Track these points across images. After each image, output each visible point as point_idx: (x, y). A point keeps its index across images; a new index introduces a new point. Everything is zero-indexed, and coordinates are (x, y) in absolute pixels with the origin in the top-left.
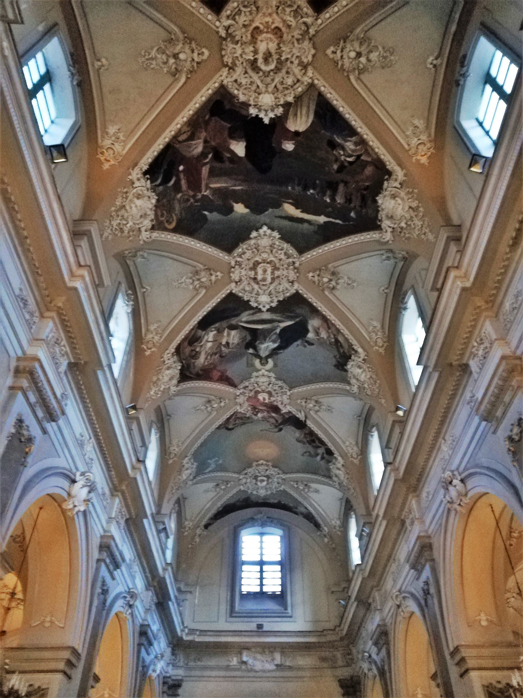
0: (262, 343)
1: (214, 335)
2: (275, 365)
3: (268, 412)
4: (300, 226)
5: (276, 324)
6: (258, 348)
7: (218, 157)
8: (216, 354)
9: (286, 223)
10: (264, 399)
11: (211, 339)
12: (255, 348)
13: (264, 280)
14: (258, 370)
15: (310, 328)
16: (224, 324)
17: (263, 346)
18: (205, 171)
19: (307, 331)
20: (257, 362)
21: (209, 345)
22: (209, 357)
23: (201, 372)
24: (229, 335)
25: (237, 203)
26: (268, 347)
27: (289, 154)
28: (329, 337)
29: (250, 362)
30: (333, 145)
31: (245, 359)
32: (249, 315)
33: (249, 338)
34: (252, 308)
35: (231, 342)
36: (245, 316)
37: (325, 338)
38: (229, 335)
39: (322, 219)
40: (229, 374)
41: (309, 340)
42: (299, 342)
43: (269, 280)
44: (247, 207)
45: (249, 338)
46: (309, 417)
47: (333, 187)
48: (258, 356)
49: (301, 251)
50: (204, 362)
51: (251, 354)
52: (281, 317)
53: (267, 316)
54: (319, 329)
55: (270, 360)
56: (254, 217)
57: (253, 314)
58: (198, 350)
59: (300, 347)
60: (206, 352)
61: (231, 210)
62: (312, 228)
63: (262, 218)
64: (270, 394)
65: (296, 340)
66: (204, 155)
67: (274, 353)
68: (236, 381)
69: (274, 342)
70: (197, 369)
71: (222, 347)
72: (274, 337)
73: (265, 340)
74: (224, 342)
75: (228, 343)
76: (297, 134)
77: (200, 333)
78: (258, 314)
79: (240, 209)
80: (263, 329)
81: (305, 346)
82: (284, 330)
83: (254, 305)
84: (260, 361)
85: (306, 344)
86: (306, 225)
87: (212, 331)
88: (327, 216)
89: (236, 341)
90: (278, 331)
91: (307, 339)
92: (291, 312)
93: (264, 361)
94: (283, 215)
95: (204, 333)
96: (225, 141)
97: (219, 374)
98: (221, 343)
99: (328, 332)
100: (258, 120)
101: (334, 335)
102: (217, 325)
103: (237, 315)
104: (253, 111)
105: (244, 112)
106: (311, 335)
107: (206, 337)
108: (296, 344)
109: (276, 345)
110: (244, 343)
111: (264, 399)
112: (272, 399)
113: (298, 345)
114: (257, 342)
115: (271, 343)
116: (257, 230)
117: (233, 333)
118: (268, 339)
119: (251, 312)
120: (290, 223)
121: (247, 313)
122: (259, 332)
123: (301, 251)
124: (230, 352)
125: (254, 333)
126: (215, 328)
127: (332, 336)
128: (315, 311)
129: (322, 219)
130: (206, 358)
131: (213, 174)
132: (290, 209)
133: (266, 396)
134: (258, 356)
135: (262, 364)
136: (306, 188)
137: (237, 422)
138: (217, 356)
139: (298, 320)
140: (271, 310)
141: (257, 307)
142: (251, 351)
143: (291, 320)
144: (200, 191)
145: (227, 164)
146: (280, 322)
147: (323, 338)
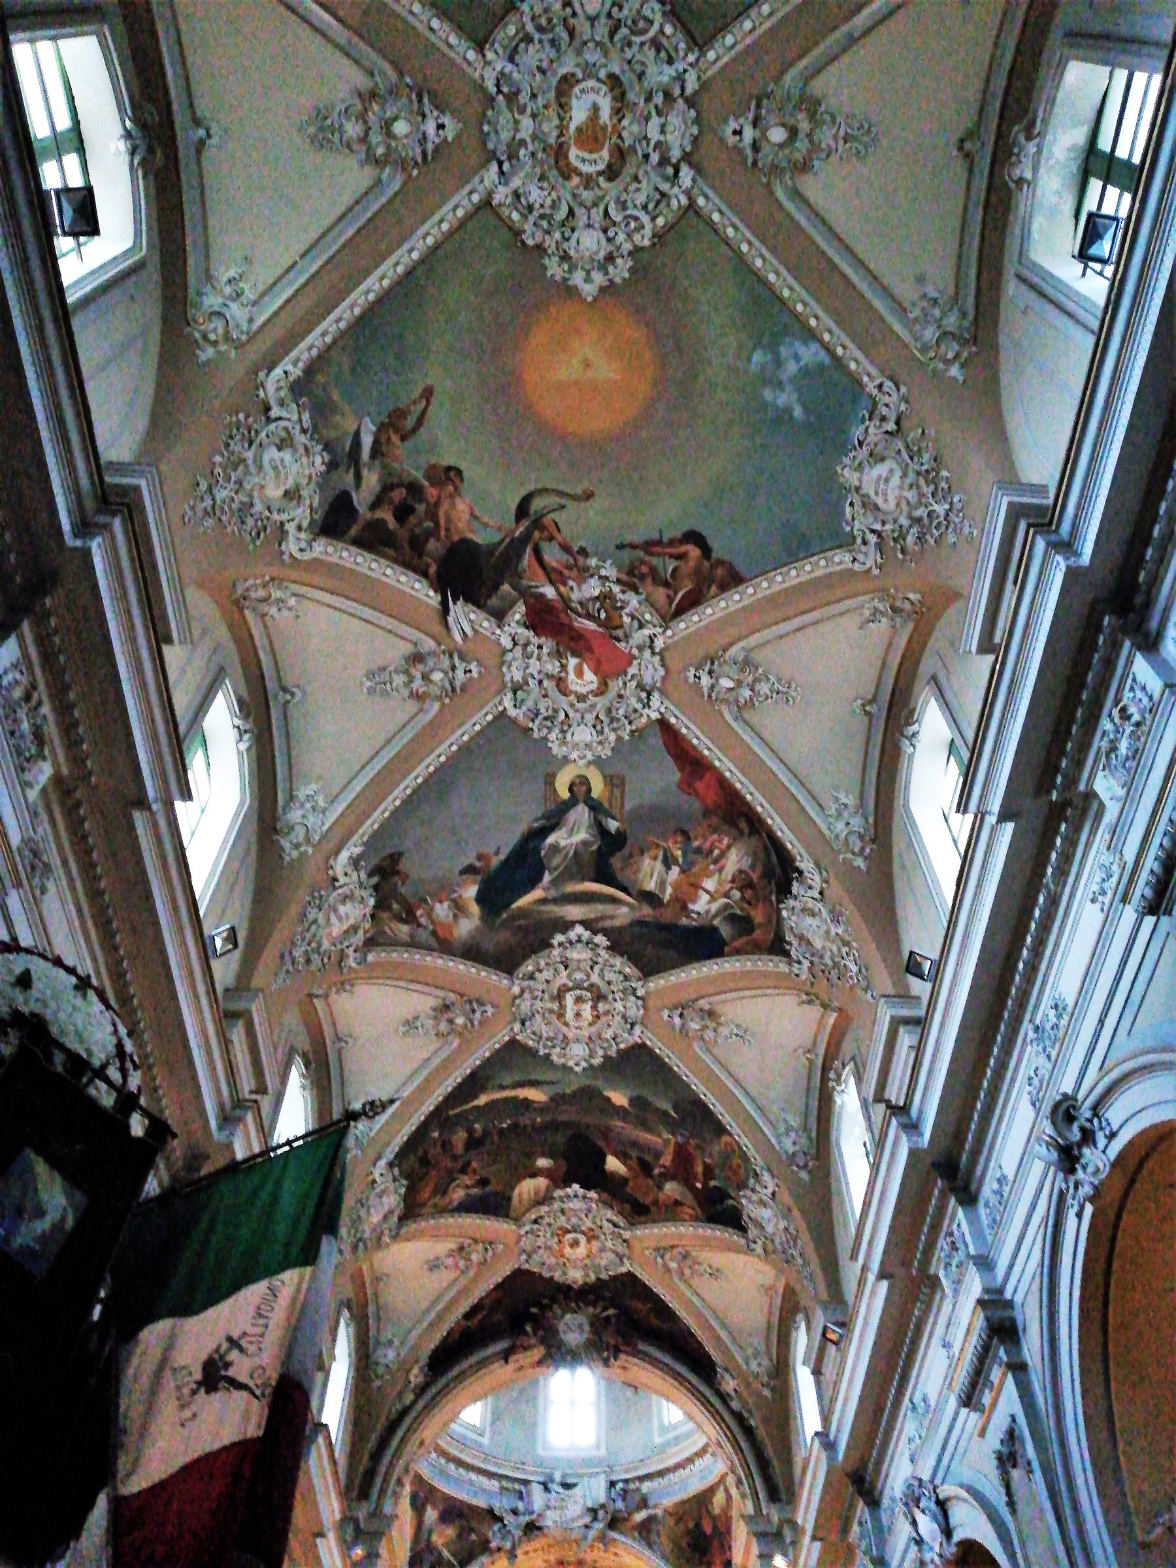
0: (585, 843)
1: (694, 902)
2: (550, 780)
3: (566, 601)
4: (517, 1078)
5: (553, 893)
6: (595, 831)
7: (645, 1168)
8: (698, 851)
9: (541, 1077)
10: (579, 673)
11: (705, 897)
12: (602, 831)
13: (579, 1000)
14: (598, 762)
15: (475, 909)
16: (667, 916)
17: (582, 835)
18: (667, 1159)
19: (480, 899)
20: (598, 788)
21: (710, 884)
22: (716, 852)
23: (743, 825)
24: (662, 884)
25: (622, 1107)
26: (570, 834)
27: (543, 1155)
28: (429, 915)
29: (617, 792)
30: (483, 1182)
31: (628, 806)
32: (612, 917)
33: (616, 862)
34: (606, 932)
35: (659, 866)
36: (622, 915)
37: (438, 905)
38: (662, 884)
39: (482, 1100)
40: (673, 774)
41: (471, 877)
42: (495, 862)
43: (569, 999)
44: (608, 1100)
45: (616, 862)
46: (437, 628)
47: (473, 1143)
48: (595, 807)
49: (513, 1043)
50: (729, 847)
51: (613, 818)
52: (540, 912)
53: (574, 912)
54: (455, 916)
55: (565, 794)
56: (599, 1083)
57: (603, 918)
58: (737, 894)
59: (492, 850)
60: (721, 870)
61: (632, 1101)
62: (497, 1081)
63: (584, 1082)
64: (561, 683)
65: (505, 863)
66: (666, 1176)
67: (554, 818)
68: (656, 740)
69: (555, 848)
70: (754, 841)
71: (681, 860)
72: (556, 861)
73: (576, 853)
74: (675, 870)
75: (668, 867)
76: (533, 1175)
77: (725, 931)
78: (592, 916)
79: (619, 1098)
80: (583, 880)
81: (480, 857)
82: (533, 881)
83: (600, 939)
84: (589, 790)
85: (478, 864)
86: (508, 1080)
87: (699, 913)
88: (477, 1108)
89: (647, 862)
90: (547, 878)
91: (479, 878)
92: (520, 928)
93: (580, 789)
94: (546, 1088)
95: (716, 922)
96: (634, 1178)
97: (699, 785)
98: (683, 871)
99: (433, 922)
100: (586, 1186)
101: (419, 925)
102: (684, 921)
103: (640, 923)
104: (593, 1194)
105: (605, 1195)
106: (471, 891)
107: (714, 907)
108: (502, 857)
109: (551, 839)
110: (626, 851)
111: (579, 673)
112: (552, 667)
113: (497, 853)
114: (595, 847)
115: (563, 843)
116: (591, 1066)
117: (651, 886)
118: (571, 853)
119: (608, 924)
120: (533, 1077)
121: (617, 923)
122: (592, 874)
123: (513, 1043)
124: (666, 840)
125: (605, 876)
126: (688, 917)
127: (423, 921)
128: (472, 953)
129: (482, 1100)
130: (723, 854)
131: (658, 1155)
132: (535, 1095)
133: (576, 684)
134: (595, 807)
135: (584, 781)
136: (515, 1127)
137: (671, 565)
138: (696, 844)
139: (504, 916)
140: (565, 926)
141: (595, 933)
142: (613, 825)
143: (519, 908)
144: (677, 1143)
145: (634, 1154)
146: (544, 901)
147: (441, 902)
